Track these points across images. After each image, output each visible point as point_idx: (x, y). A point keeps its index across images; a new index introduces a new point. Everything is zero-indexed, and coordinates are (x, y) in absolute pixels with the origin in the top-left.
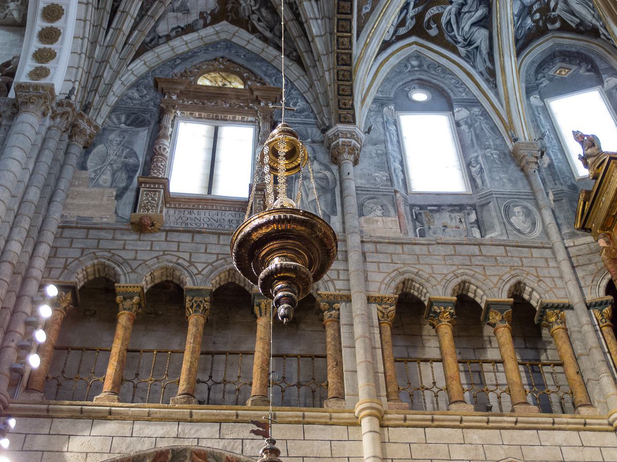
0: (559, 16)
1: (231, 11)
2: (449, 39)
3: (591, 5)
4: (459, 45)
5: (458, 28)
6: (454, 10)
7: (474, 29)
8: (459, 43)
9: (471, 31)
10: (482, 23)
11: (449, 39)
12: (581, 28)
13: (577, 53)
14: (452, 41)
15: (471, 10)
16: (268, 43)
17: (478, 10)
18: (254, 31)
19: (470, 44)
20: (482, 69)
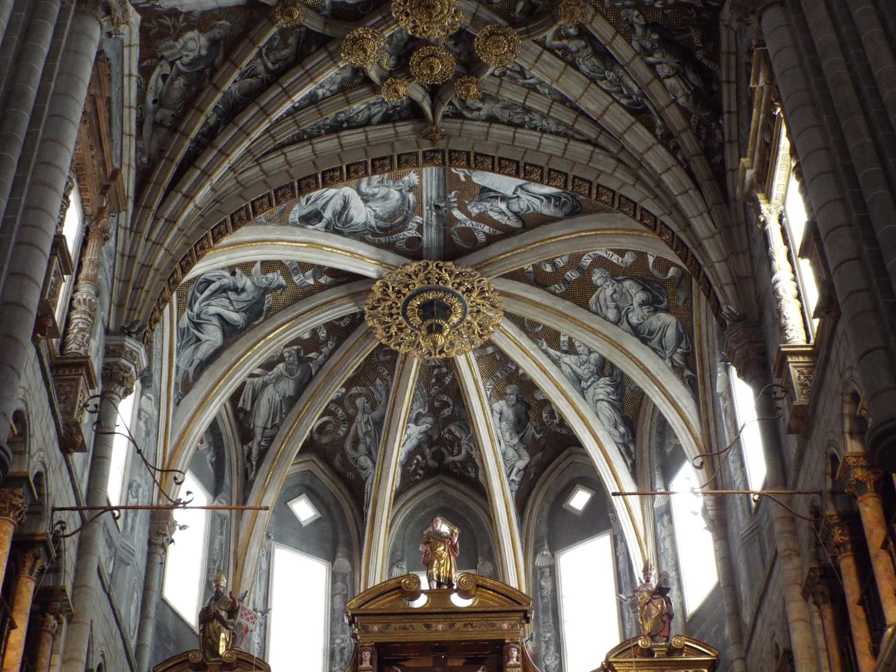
1: (161, 25)
3: (277, 421)
4: (190, 313)
5: (208, 298)
6: (225, 281)
7: (215, 321)
8: (192, 310)
9: (212, 318)
10: (227, 329)
11: (190, 293)
12: (241, 415)
14: (189, 299)
15: (234, 303)
16: (137, 106)
17: (237, 312)
18: (145, 72)
19: (198, 326)
20: (183, 367)
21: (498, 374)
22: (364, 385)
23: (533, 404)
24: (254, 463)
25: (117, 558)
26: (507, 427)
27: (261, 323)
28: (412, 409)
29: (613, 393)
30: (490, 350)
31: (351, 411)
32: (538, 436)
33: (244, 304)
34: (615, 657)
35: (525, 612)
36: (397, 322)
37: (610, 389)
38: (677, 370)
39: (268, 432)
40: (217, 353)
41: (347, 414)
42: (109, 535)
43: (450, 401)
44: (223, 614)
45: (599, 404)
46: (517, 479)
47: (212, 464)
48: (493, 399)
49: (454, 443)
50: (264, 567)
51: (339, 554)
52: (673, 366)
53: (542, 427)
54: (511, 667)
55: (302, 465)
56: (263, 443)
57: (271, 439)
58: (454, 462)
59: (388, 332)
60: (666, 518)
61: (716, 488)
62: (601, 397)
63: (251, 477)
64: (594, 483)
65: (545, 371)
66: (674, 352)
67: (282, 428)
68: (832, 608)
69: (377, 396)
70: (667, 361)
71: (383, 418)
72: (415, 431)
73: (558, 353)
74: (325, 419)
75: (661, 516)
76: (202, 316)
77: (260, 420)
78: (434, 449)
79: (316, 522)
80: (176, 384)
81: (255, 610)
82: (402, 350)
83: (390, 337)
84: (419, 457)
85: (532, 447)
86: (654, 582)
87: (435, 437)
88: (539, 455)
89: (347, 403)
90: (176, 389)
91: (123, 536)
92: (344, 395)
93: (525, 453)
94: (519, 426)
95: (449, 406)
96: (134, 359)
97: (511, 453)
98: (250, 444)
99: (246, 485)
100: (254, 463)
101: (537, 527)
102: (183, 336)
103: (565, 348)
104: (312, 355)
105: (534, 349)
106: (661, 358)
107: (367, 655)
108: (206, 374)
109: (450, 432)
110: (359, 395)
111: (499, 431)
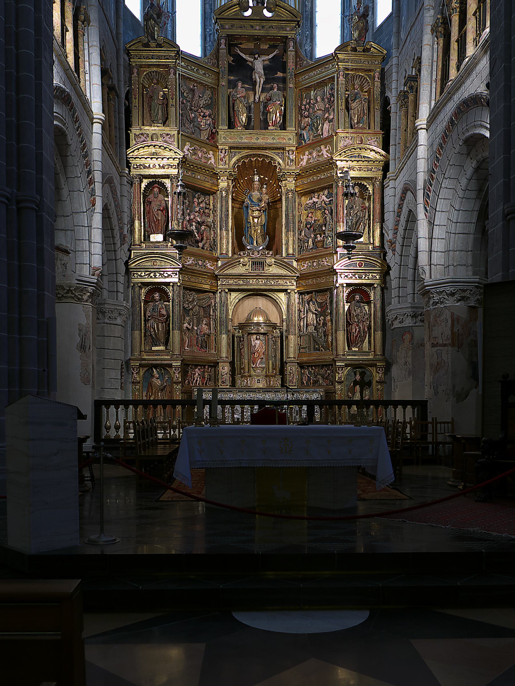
34: (339, 51)
35: (298, 22)
44: (155, 16)
68: (443, 40)
86: (362, 10)
107: (223, 41)
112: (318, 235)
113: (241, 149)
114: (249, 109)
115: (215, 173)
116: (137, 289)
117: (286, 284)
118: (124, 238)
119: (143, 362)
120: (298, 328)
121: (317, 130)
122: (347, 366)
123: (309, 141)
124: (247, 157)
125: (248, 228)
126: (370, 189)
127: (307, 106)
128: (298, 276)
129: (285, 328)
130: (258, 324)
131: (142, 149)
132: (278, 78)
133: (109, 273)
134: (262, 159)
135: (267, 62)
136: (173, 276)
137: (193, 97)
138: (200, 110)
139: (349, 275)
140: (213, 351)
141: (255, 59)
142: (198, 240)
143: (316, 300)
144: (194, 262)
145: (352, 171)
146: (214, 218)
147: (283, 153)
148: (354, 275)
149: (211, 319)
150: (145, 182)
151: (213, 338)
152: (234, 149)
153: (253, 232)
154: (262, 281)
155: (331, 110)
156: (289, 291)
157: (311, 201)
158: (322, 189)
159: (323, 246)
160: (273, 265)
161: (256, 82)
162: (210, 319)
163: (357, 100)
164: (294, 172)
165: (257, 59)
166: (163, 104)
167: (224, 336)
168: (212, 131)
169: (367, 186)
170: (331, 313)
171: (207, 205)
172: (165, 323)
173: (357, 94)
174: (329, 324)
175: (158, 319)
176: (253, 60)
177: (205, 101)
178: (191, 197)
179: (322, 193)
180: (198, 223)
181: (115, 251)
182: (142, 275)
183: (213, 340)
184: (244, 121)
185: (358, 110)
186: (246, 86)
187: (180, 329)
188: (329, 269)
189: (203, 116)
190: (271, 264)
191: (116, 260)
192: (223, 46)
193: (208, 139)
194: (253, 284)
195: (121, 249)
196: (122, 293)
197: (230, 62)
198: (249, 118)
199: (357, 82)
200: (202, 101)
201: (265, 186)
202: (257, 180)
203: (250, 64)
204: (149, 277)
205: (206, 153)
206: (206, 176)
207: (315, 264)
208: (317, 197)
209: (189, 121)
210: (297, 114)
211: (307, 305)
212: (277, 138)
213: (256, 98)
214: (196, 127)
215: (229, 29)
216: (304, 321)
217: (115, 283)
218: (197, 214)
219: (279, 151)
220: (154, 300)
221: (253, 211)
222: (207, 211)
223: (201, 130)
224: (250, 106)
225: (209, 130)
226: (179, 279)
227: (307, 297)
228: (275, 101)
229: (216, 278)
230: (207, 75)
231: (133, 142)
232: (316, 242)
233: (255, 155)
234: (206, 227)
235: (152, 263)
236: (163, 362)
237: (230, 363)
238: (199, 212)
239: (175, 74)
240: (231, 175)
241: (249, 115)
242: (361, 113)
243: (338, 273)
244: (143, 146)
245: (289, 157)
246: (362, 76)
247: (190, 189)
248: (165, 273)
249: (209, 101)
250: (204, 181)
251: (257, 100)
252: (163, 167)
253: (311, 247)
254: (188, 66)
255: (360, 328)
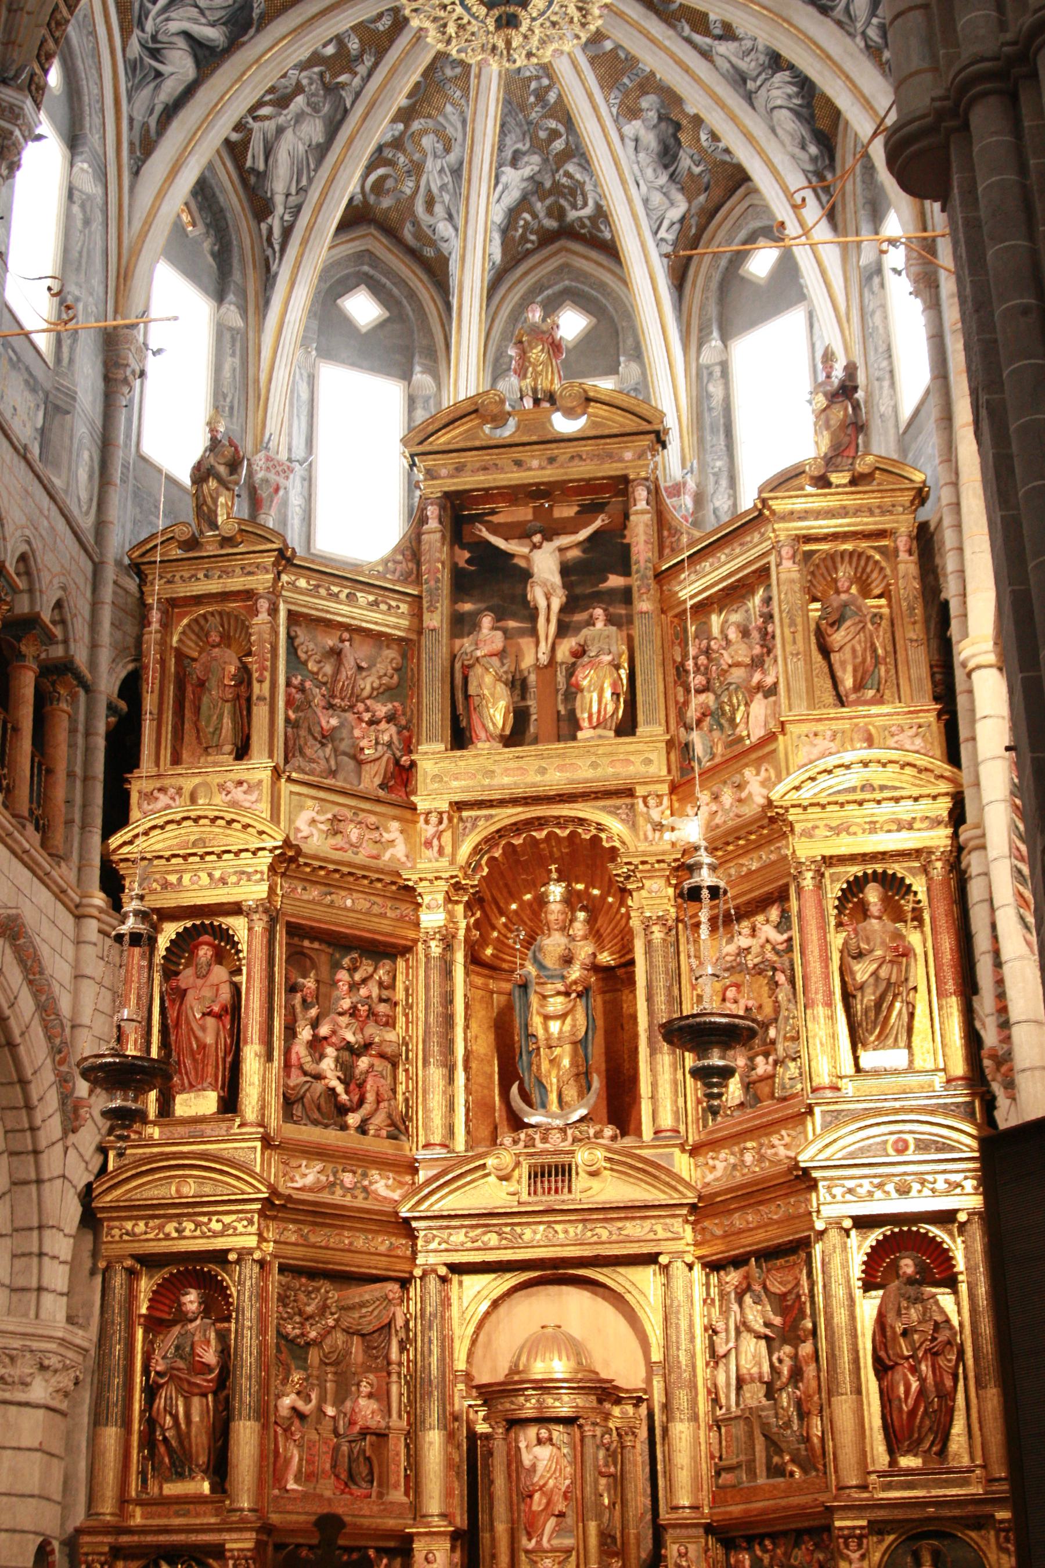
0: (251, 131)
2: (137, 6)
3: (304, 182)
4: (140, 34)
7: (181, 43)
8: (143, 30)
9: (175, 39)
10: (200, 53)
12: (253, 180)
13: (222, 210)
15: (207, 13)
17: (213, 26)
19: (155, 54)
20: (139, 118)
21: (626, 80)
22: (429, 116)
23: (684, 122)
24: (277, 247)
25: (50, 405)
26: (649, 160)
27: (252, 38)
28: (500, 150)
29: (797, 95)
30: (608, 45)
31: (416, 157)
32: (697, 170)
33: (223, 13)
34: (771, 491)
36: (455, 16)
37: (792, 90)
38: (873, 52)
39: (293, 200)
40: (189, 92)
41: (411, 161)
42: (31, 374)
43: (561, 128)
44: (222, 470)
45: (776, 112)
46: (670, 237)
47: (213, 254)
48: (621, 119)
49: (574, 192)
50: (305, 396)
51: (417, 369)
52: (868, 47)
53: (702, 156)
54: (637, 513)
55: (357, 243)
56: (287, 217)
57: (297, 210)
58: (580, 219)
59: (444, 33)
60: (876, 280)
61: (925, 230)
62: (779, 102)
63: (274, 268)
64: (773, 232)
65: (687, 70)
66: (868, 23)
67: (310, 193)
69: (450, 131)
70: (858, 39)
71: (461, 163)
72: (515, 179)
73: (708, 40)
74: (381, 171)
75: (870, 278)
76: (160, 37)
77: (280, 184)
78: (548, 202)
79: (382, 325)
80: (131, 144)
81: (290, 460)
82: (473, 59)
83: (449, 42)
84: (527, 216)
85: (689, 186)
87: (548, 184)
88: (702, 198)
89: (409, 146)
90: (132, 151)
91: (57, 374)
92: (403, 134)
93: (679, 198)
94: (667, 156)
95: (560, 136)
96: (17, 117)
97: (657, 198)
98: (269, 220)
99: (267, 279)
100: (277, 247)
101: (702, 308)
102: (134, 70)
103: (718, 31)
104: (343, 78)
105: (669, 38)
106: (850, 34)
107: (432, 511)
108: (175, 124)
109: (568, 174)
110: (424, 132)
111: (635, 167)
112: (760, 1060)
113: (492, 806)
114: (518, 685)
115: (407, 888)
116: (118, 1280)
117: (651, 1236)
118: (76, 1109)
119: (124, 1539)
120: (709, 1392)
121: (732, 721)
122: (877, 1528)
123: (710, 760)
124: (517, 828)
125: (530, 1053)
126: (919, 885)
127: (702, 660)
128: (693, 1208)
129: (658, 1397)
130: (544, 1387)
131: (158, 831)
132: (612, 592)
133: (17, 1225)
134: (568, 832)
135: (575, 553)
136: (240, 1229)
137: (337, 672)
138: (361, 707)
139: (861, 1186)
140: (398, 1496)
141: (535, 547)
142: (344, 1105)
143: (765, 1287)
144: (323, 1178)
145: (844, 834)
146: (407, 1030)
147: (633, 805)
148: (880, 1186)
149: (394, 1378)
150: (170, 931)
151: (397, 1446)
152: (472, 809)
153: (545, 1065)
154: (566, 1232)
155: (768, 661)
156: (663, 1260)
157: (731, 948)
158: (761, 905)
159: (772, 1096)
160: (607, 1173)
161: (536, 608)
162: (389, 1374)
163: (848, 623)
164: (663, 861)
165: (540, 547)
166: (238, 697)
167: (434, 1441)
168: (397, 762)
169: (908, 882)
170: (814, 1332)
171: (386, 988)
172: (215, 1393)
173: (845, 605)
174: (810, 1371)
175: (189, 1383)
176: (525, 550)
177: (380, 678)
178: (325, 969)
179: (760, 918)
180: (348, 1047)
181: (36, 1152)
182: (137, 1230)
183: (398, 1454)
184: (500, 724)
185: (854, 650)
186: (512, 624)
187: (264, 1413)
188: (790, 1170)
189: (371, 723)
190: (594, 1168)
191: (39, 1182)
192: (433, 524)
193: (382, 786)
194: (535, 1243)
195: (66, 1149)
196: (62, 1294)
197: (462, 564)
198: (520, 717)
199: (844, 573)
200: (369, 680)
201: (581, 915)
202: (558, 899)
203: (522, 563)
204: (161, 1236)
205: (377, 828)
206: (373, 898)
207: (748, 1158)
208: (746, 931)
209: (315, 739)
210: (672, 685)
211: (735, 1307)
212: (606, 760)
213: (540, 655)
214: (345, 754)
215: (452, 477)
216: (727, 1365)
217: (35, 1260)
218: (344, 1020)
219: (618, 802)
220: (182, 1318)
221: (545, 997)
222: (382, 1008)
223: (360, 763)
224: (524, 681)
225: (385, 759)
226: (262, 1238)
227: (733, 1277)
228: (597, 656)
229: (405, 1228)
230: (384, 607)
231: (135, 814)
232: (754, 1083)
233: (540, 822)
234: (377, 1062)
235: (173, 1189)
236: (193, 1538)
237: (455, 1536)
238: (353, 1012)
239: (273, 611)
240: (457, 887)
241: (522, 704)
242: (864, 661)
243: (821, 1184)
244: (160, 822)
245: (648, 813)
246: (860, 555)
247: (321, 941)
248: (214, 1218)
249: (392, 677)
250: (368, 913)
251: (544, 659)
252: (223, 881)
253: (737, 1102)
254: (317, 586)
255: (922, 1380)
